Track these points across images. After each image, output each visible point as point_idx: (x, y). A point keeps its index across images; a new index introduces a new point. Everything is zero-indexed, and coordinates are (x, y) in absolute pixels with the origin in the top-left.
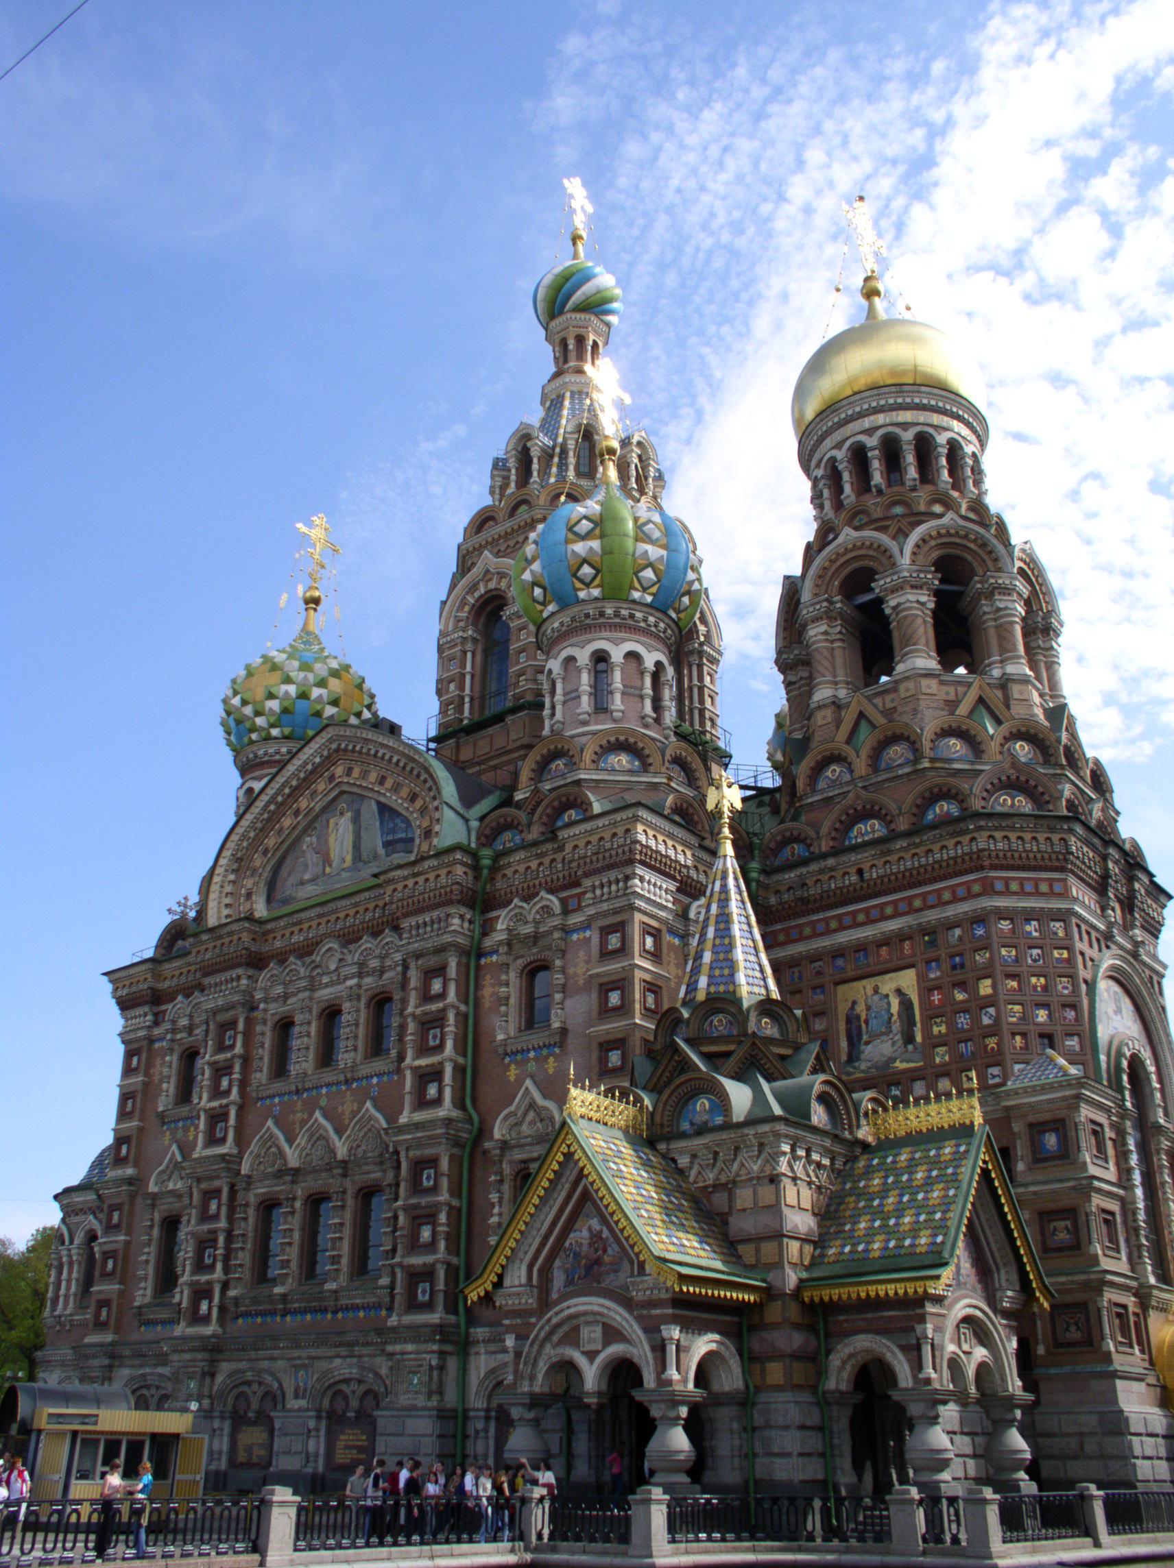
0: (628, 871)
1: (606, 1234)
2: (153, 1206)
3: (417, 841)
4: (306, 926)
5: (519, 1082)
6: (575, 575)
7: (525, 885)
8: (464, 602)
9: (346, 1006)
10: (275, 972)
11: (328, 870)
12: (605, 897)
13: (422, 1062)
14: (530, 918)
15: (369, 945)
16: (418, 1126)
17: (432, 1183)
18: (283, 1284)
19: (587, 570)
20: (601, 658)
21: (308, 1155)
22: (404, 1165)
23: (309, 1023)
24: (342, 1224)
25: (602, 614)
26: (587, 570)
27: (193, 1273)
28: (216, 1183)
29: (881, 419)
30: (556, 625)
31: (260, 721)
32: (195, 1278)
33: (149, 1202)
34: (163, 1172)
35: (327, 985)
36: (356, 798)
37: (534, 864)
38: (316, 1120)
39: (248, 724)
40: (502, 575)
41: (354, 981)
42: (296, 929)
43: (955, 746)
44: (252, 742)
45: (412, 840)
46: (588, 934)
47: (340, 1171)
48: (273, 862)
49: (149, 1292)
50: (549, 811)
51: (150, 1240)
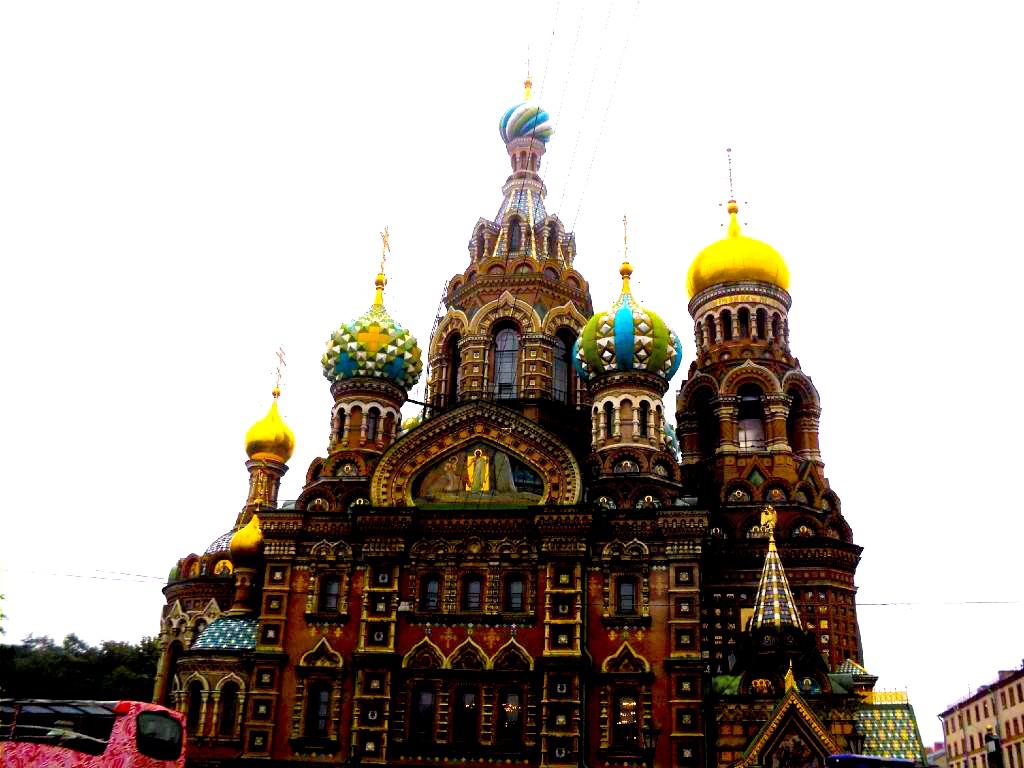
0: (698, 541)
1: (803, 743)
3: (547, 488)
5: (618, 642)
8: (486, 318)
11: (468, 488)
12: (681, 552)
13: (559, 622)
19: (642, 353)
20: (644, 405)
25: (646, 380)
26: (642, 353)
29: (758, 299)
30: (617, 377)
31: (370, 364)
32: (363, 728)
35: (470, 561)
36: (491, 449)
39: (361, 364)
40: (517, 310)
41: (497, 563)
43: (803, 498)
44: (358, 375)
45: (542, 487)
46: (664, 568)
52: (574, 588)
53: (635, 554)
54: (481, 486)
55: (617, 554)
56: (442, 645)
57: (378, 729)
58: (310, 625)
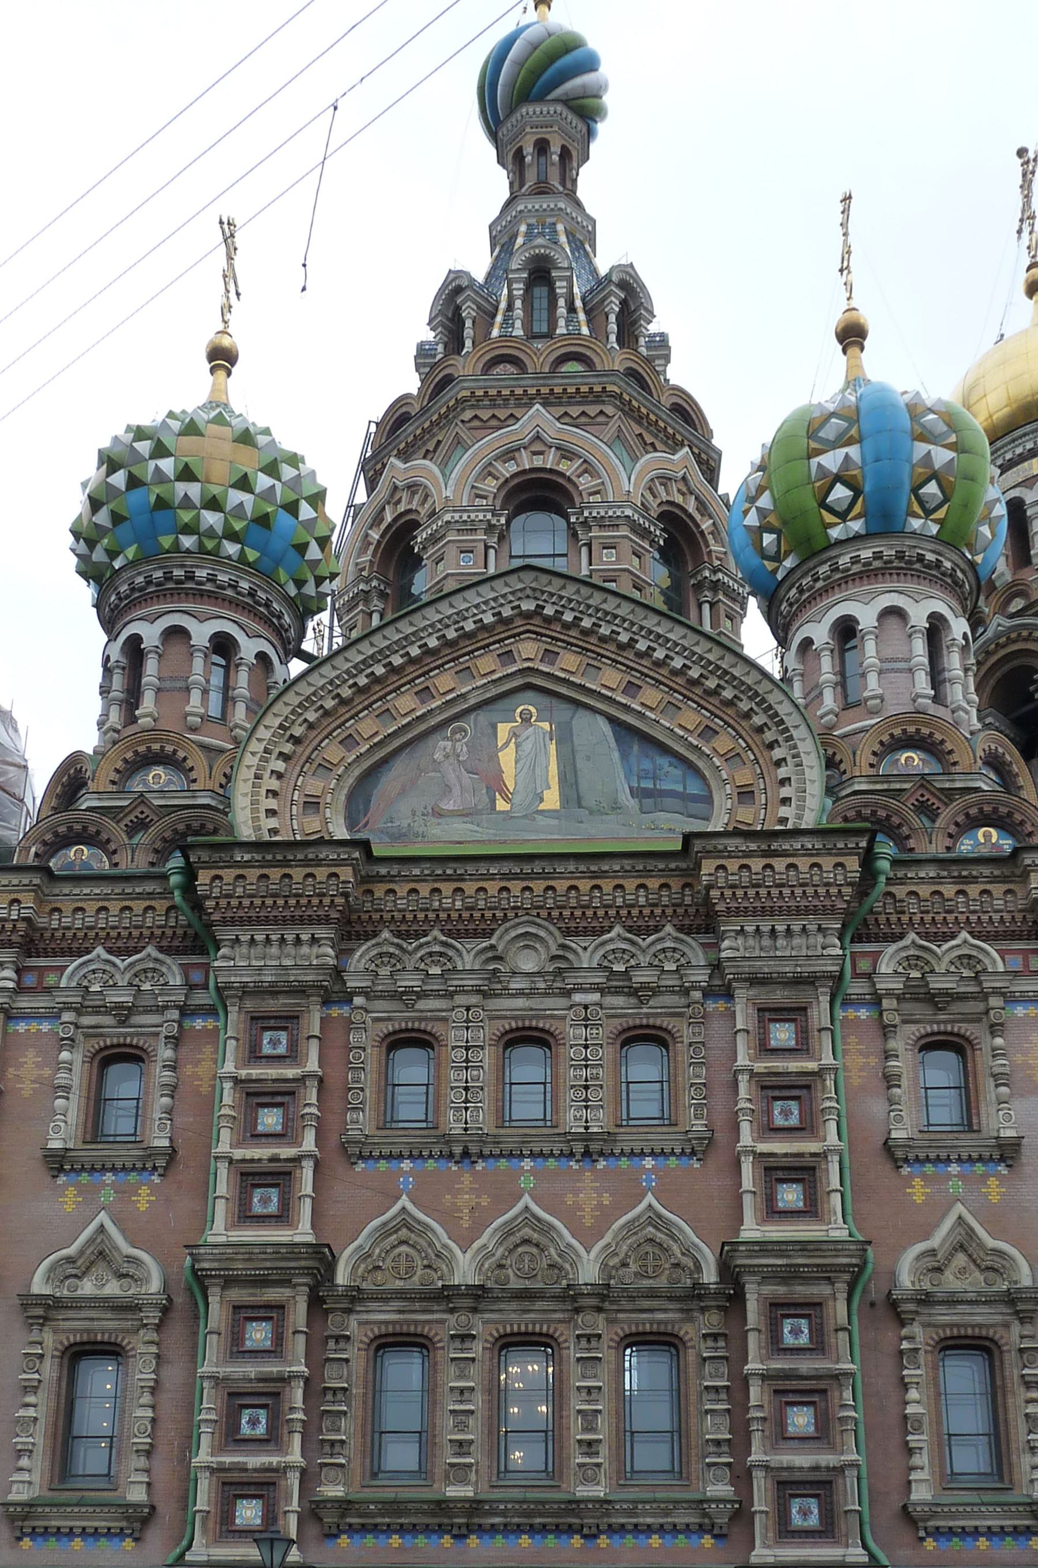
2: (46, 1319)
4: (470, 887)
6: (915, 490)
7: (928, 918)
9: (575, 1034)
10: (392, 950)
11: (501, 805)
14: (940, 968)
15: (624, 946)
16: (804, 1246)
17: (804, 1340)
18: (464, 1481)
21: (501, 1266)
22: (752, 1306)
23: (482, 1048)
24: (600, 1388)
27: (216, 1450)
28: (273, 1295)
32: (228, 1459)
33: (39, 1311)
34: (70, 1260)
35: (520, 993)
37: (949, 890)
38: (527, 1208)
41: (596, 997)
42: (447, 888)
47: (593, 1302)
48: (366, 764)
49: (36, 1478)
50: (960, 819)
51: (40, 1381)
52: (812, 1058)
53: (966, 973)
54: (542, 800)
55: (915, 974)
56: (448, 1219)
57: (274, 1460)
58: (62, 1179)
